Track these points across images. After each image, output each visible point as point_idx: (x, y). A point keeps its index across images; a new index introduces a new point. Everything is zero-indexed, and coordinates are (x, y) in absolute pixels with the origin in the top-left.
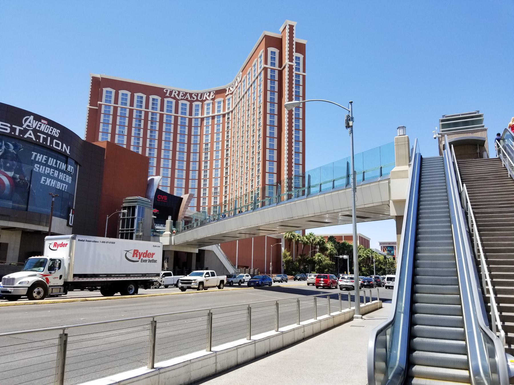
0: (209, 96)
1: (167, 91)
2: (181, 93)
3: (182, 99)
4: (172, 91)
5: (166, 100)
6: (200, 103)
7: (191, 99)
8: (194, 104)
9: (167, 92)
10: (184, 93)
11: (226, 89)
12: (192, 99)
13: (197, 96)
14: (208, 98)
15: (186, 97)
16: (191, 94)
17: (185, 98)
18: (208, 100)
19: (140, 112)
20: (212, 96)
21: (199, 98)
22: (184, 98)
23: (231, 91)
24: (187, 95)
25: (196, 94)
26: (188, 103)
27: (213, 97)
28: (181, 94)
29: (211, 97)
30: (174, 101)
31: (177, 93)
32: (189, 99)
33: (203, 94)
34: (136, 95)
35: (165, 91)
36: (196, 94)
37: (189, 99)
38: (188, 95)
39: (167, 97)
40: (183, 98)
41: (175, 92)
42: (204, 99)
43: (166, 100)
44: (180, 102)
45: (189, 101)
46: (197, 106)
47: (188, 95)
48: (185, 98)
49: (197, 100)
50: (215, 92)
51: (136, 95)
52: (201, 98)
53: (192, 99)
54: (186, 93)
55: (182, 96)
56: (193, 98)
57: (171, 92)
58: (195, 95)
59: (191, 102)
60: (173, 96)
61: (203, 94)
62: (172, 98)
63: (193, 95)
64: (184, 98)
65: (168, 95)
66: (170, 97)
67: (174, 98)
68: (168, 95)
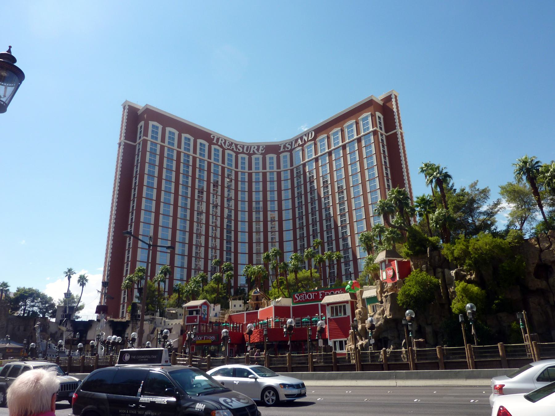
0: (258, 150)
1: (214, 137)
2: (227, 142)
3: (228, 149)
4: (219, 138)
5: (213, 147)
7: (236, 150)
8: (240, 156)
9: (214, 139)
10: (230, 143)
11: (280, 145)
12: (237, 150)
13: (243, 148)
14: (256, 152)
16: (236, 145)
17: (231, 149)
18: (256, 154)
19: (188, 156)
20: (262, 150)
22: (230, 148)
23: (288, 148)
25: (242, 146)
26: (234, 154)
28: (227, 143)
29: (260, 151)
30: (221, 150)
31: (224, 141)
32: (235, 150)
33: (250, 147)
35: (212, 136)
36: (242, 146)
37: (235, 150)
38: (233, 145)
39: (214, 144)
40: (229, 148)
41: (222, 140)
42: (252, 152)
43: (213, 147)
44: (227, 152)
45: (235, 152)
46: (243, 159)
47: (233, 145)
48: (231, 149)
49: (243, 153)
50: (265, 146)
51: (184, 135)
52: (247, 150)
53: (237, 150)
54: (232, 143)
55: (228, 146)
56: (240, 150)
57: (218, 139)
58: (240, 146)
59: (237, 153)
60: (219, 144)
61: (250, 147)
62: (219, 145)
63: (238, 147)
64: (230, 148)
65: (215, 141)
66: (217, 144)
67: (221, 146)
68: (215, 141)
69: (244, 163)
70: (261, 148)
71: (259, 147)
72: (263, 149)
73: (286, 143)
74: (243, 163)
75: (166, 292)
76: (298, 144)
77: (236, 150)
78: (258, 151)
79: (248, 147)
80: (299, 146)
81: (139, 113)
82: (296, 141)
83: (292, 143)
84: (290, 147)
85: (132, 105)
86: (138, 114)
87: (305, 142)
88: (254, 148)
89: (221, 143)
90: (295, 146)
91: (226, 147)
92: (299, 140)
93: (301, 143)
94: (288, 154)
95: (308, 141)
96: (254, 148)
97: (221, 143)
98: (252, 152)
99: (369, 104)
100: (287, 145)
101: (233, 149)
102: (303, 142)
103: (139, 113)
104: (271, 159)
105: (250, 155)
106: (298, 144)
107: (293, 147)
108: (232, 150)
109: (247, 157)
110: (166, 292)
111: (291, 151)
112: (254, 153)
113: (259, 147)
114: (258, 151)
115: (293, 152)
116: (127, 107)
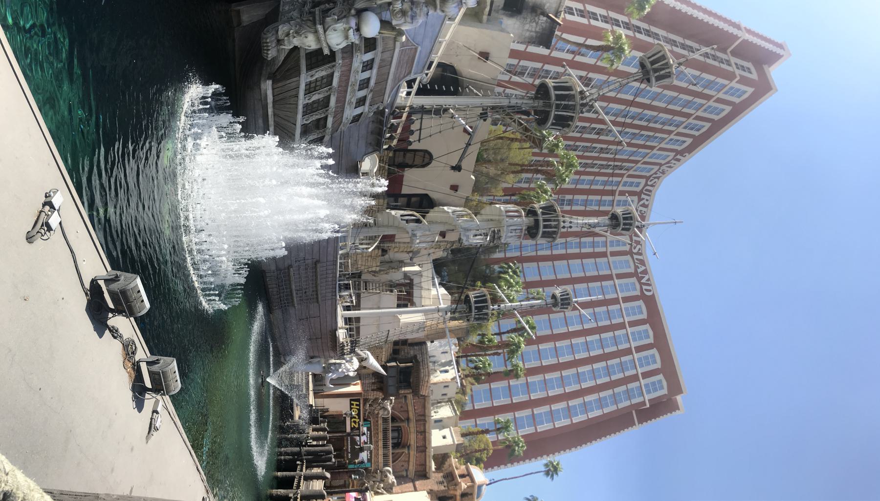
0: (644, 206)
3: (659, 169)
13: (652, 186)
14: (642, 202)
16: (658, 178)
20: (641, 211)
21: (648, 188)
26: (648, 174)
32: (654, 176)
34: (707, 125)
37: (654, 176)
39: (675, 156)
40: (661, 171)
47: (661, 175)
49: (646, 185)
50: (645, 215)
52: (647, 190)
53: (651, 178)
56: (650, 181)
59: (647, 178)
62: (671, 160)
63: (656, 180)
67: (668, 162)
68: (679, 157)
69: (631, 186)
70: (644, 209)
71: (646, 206)
72: (643, 212)
73: (641, 245)
74: (631, 184)
76: (639, 265)
78: (641, 206)
79: (650, 191)
80: (636, 267)
81: (765, 67)
82: (642, 262)
83: (641, 254)
84: (635, 251)
85: (780, 61)
86: (765, 65)
87: (639, 279)
88: (647, 200)
90: (636, 261)
91: (664, 167)
92: (643, 268)
93: (639, 271)
94: (627, 248)
95: (641, 284)
96: (647, 200)
98: (643, 196)
99: (675, 387)
100: (639, 247)
102: (640, 275)
103: (765, 67)
105: (638, 194)
106: (639, 265)
107: (635, 257)
108: (656, 173)
109: (638, 189)
111: (630, 253)
112: (640, 199)
113: (646, 206)
114: (641, 206)
115: (629, 255)
116: (778, 51)
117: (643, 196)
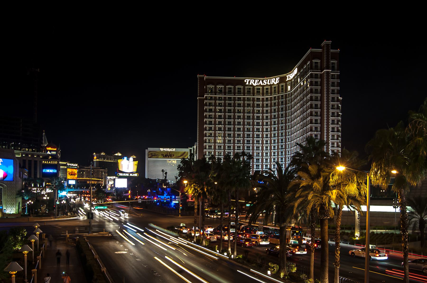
6: (269, 87)
7: (263, 84)
9: (247, 82)
13: (267, 82)
15: (260, 83)
24: (260, 82)
27: (278, 82)
40: (257, 84)
50: (279, 78)
52: (269, 83)
53: (264, 84)
55: (257, 83)
56: (265, 83)
58: (265, 81)
60: (251, 84)
63: (264, 81)
65: (247, 84)
68: (247, 84)
75: (129, 175)
77: (263, 84)
89: (252, 83)
97: (252, 83)
101: (260, 84)
104: (282, 86)
110: (129, 175)
117: (272, 83)
